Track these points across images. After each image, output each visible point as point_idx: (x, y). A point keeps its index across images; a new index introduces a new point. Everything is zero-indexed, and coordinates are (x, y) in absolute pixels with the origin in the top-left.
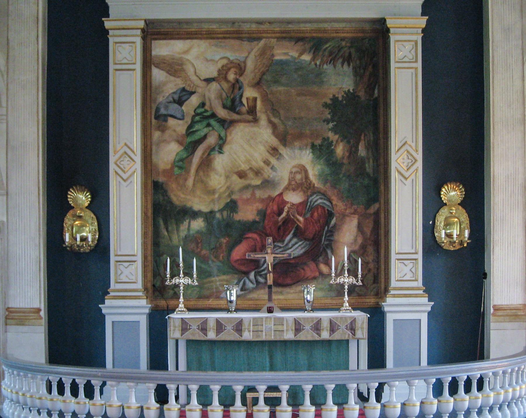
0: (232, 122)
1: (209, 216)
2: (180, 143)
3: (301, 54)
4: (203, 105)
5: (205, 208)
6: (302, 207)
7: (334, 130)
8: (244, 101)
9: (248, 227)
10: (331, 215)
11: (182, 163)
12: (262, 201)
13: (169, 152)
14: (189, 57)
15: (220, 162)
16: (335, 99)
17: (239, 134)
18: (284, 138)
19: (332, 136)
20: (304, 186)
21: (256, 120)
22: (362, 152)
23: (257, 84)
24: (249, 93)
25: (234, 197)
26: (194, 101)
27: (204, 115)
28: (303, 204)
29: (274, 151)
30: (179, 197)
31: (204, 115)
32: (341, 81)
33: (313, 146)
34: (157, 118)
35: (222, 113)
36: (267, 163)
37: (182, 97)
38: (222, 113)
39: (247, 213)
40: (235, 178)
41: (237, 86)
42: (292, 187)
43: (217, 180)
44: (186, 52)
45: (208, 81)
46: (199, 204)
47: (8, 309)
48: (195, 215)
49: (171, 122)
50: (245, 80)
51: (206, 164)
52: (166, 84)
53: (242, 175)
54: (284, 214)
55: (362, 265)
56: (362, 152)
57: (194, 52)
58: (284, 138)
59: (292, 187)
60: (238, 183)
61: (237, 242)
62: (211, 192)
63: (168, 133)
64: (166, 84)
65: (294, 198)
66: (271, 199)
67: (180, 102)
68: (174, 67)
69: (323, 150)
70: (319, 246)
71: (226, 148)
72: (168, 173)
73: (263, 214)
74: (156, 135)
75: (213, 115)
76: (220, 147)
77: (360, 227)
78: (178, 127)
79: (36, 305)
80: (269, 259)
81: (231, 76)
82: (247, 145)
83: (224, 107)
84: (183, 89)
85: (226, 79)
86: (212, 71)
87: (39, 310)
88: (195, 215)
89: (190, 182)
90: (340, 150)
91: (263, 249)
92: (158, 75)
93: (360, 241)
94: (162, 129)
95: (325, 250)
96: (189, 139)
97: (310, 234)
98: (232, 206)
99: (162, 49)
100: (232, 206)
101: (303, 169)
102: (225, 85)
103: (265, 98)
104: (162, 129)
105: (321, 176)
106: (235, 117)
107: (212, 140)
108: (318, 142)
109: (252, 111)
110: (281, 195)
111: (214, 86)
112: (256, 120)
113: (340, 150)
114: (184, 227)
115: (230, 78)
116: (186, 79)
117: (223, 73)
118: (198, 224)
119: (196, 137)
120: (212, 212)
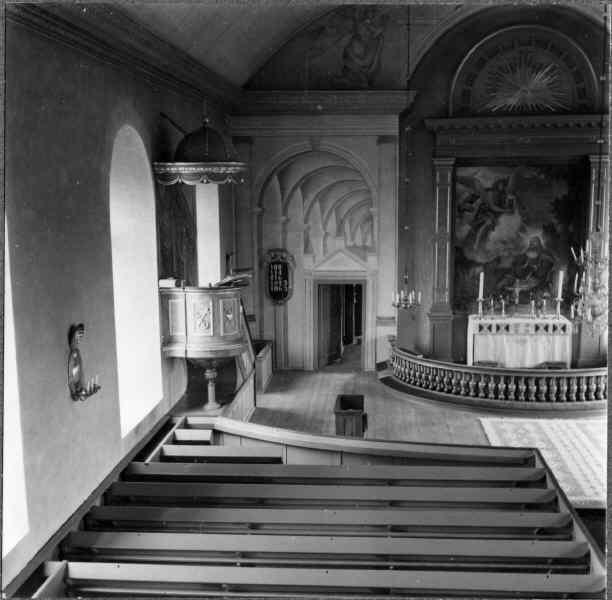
0: (500, 214)
2: (470, 225)
3: (539, 174)
4: (484, 204)
7: (556, 217)
8: (507, 201)
9: (508, 271)
10: (552, 265)
11: (471, 236)
12: (516, 257)
14: (476, 177)
15: (493, 235)
16: (557, 200)
17: (503, 220)
18: (527, 222)
19: (555, 221)
25: (501, 254)
26: (479, 201)
28: (538, 258)
29: (522, 229)
30: (469, 255)
31: (484, 210)
32: (561, 190)
33: (544, 227)
34: (459, 210)
35: (496, 209)
36: (519, 236)
37: (473, 199)
38: (496, 209)
39: (506, 264)
43: (489, 246)
44: (476, 173)
45: (488, 190)
46: (480, 259)
47: (379, 318)
49: (467, 213)
50: (507, 189)
51: (485, 237)
52: (465, 193)
53: (504, 243)
54: (526, 265)
56: (571, 228)
58: (527, 222)
59: (532, 249)
60: (501, 246)
61: (500, 280)
62: (487, 252)
64: (465, 193)
65: (532, 255)
67: (472, 202)
68: (469, 182)
69: (549, 230)
70: (545, 283)
71: (496, 228)
73: (514, 264)
74: (458, 220)
76: (492, 227)
78: (470, 215)
80: (517, 291)
81: (501, 187)
82: (507, 225)
83: (495, 204)
84: (473, 195)
85: (497, 188)
86: (489, 184)
87: (394, 318)
89: (475, 247)
92: (460, 187)
94: (461, 217)
95: (548, 283)
97: (540, 275)
98: (498, 260)
99: (463, 172)
100: (498, 260)
101: (538, 239)
102: (497, 193)
103: (518, 199)
105: (547, 244)
107: (489, 222)
109: (511, 206)
111: (490, 193)
113: (559, 229)
115: (499, 189)
117: (495, 187)
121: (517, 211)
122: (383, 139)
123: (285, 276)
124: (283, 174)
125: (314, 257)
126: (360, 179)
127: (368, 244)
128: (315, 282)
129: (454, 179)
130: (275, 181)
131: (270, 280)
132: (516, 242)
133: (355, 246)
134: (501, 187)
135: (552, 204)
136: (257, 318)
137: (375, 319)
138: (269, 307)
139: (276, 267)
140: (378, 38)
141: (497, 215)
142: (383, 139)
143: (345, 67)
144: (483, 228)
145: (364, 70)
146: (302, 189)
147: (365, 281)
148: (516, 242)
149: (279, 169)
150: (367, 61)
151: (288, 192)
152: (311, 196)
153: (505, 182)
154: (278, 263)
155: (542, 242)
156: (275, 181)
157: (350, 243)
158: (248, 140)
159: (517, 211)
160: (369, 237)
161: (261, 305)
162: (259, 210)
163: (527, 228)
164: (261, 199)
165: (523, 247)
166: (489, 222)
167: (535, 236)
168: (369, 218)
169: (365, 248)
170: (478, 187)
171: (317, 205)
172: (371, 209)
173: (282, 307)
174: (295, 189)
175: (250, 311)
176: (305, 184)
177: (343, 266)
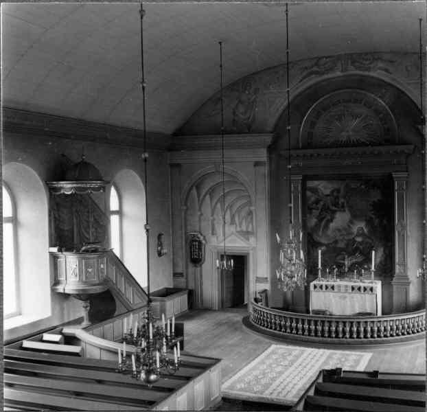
1: (327, 245)
2: (316, 218)
3: (361, 185)
5: (326, 242)
6: (361, 243)
9: (342, 250)
11: (317, 226)
14: (319, 187)
15: (332, 225)
19: (373, 216)
20: (363, 235)
21: (344, 211)
23: (344, 198)
24: (342, 200)
25: (337, 238)
26: (322, 203)
28: (363, 241)
29: (351, 222)
30: (317, 238)
31: (326, 209)
32: (376, 196)
33: (366, 220)
35: (334, 208)
36: (349, 226)
37: (317, 202)
38: (334, 208)
39: (341, 245)
40: (337, 231)
41: (337, 197)
42: (358, 235)
43: (329, 232)
45: (328, 195)
46: (323, 241)
47: (257, 278)
49: (314, 211)
51: (326, 226)
53: (339, 230)
55: (318, 256)
56: (385, 222)
57: (322, 185)
59: (358, 235)
60: (338, 234)
65: (359, 239)
66: (350, 240)
67: (317, 204)
68: (314, 190)
69: (369, 222)
73: (347, 245)
74: (308, 215)
76: (331, 221)
77: (384, 251)
79: (265, 276)
81: (335, 194)
82: (341, 219)
83: (332, 205)
86: (328, 192)
87: (267, 278)
89: (320, 233)
90: (377, 221)
91: (344, 259)
92: (309, 193)
94: (311, 213)
98: (336, 242)
99: (310, 184)
100: (336, 242)
103: (348, 203)
105: (369, 231)
108: (368, 218)
109: (343, 207)
110: (353, 238)
111: (329, 198)
112: (344, 211)
115: (335, 193)
116: (319, 196)
117: (332, 192)
119: (323, 216)
120: (329, 244)
121: (346, 209)
122: (257, 164)
123: (200, 249)
124: (198, 188)
125: (217, 237)
126: (243, 189)
127: (250, 230)
128: (218, 253)
129: (304, 189)
130: (194, 192)
131: (191, 252)
132: (348, 230)
133: (242, 231)
134: (335, 194)
135: (370, 205)
137: (255, 279)
138: (191, 268)
139: (194, 243)
140: (253, 102)
141: (334, 212)
142: (257, 164)
143: (234, 120)
146: (210, 194)
147: (248, 254)
148: (348, 230)
149: (196, 184)
150: (248, 115)
151: (201, 197)
152: (215, 201)
153: (338, 191)
154: (196, 241)
155: (365, 230)
156: (194, 192)
157: (239, 229)
158: (178, 165)
159: (346, 209)
160: (251, 226)
161: (187, 267)
162: (185, 208)
163: (355, 222)
164: (187, 199)
165: (352, 234)
166: (329, 217)
167: (359, 226)
168: (250, 213)
170: (320, 194)
173: (199, 269)
174: (205, 196)
175: (179, 270)
176: (212, 192)
177: (236, 244)
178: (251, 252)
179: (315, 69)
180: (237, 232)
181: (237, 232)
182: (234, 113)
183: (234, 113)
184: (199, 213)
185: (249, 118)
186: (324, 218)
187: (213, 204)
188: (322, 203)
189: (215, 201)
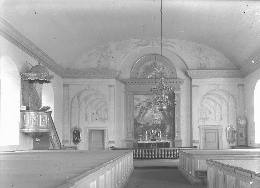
1: (144, 125)
11: (139, 116)
13: (137, 114)
15: (146, 115)
22: (170, 114)
27: (143, 108)
30: (138, 122)
35: (147, 108)
38: (147, 108)
39: (150, 124)
43: (145, 119)
46: (142, 123)
48: (141, 125)
51: (143, 116)
56: (170, 114)
57: (141, 97)
63: (137, 111)
64: (136, 102)
67: (139, 106)
68: (138, 100)
72: (137, 118)
74: (135, 111)
75: (145, 108)
76: (145, 113)
77: (170, 127)
83: (147, 106)
86: (144, 100)
88: (141, 125)
92: (135, 101)
93: (170, 129)
94: (136, 110)
96: (140, 112)
99: (136, 97)
104: (136, 110)
106: (149, 108)
111: (145, 103)
114: (140, 127)
117: (147, 100)
118: (142, 126)
119: (142, 111)
122: (110, 86)
124: (78, 97)
125: (88, 122)
127: (106, 118)
128: (88, 129)
133: (101, 118)
136: (69, 141)
141: (147, 109)
142: (110, 86)
144: (142, 113)
145: (105, 66)
152: (88, 103)
157: (100, 117)
160: (106, 115)
164: (72, 103)
166: (144, 112)
168: (106, 109)
169: (105, 119)
171: (89, 106)
172: (107, 107)
176: (86, 98)
177: (98, 124)
178: (106, 129)
179: (140, 43)
180: (99, 119)
181: (99, 119)
182: (99, 61)
183: (99, 61)
184: (78, 110)
185: (107, 64)
186: (142, 112)
187: (87, 105)
188: (141, 106)
189: (88, 103)
